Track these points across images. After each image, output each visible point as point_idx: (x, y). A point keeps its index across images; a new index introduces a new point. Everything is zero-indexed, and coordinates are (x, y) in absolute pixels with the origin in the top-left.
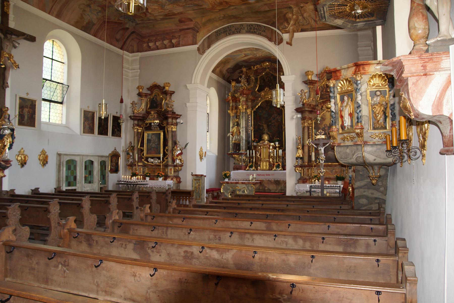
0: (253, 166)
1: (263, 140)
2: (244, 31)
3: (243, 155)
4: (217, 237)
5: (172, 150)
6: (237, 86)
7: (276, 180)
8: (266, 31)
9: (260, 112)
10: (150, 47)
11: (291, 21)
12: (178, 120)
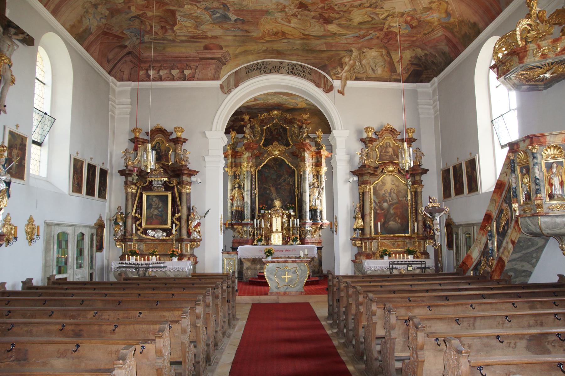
0: (262, 240)
1: (275, 207)
2: (284, 71)
3: (249, 226)
4: (539, 322)
5: (188, 220)
6: (237, 138)
8: (313, 74)
10: (149, 76)
11: (345, 67)
12: (193, 178)
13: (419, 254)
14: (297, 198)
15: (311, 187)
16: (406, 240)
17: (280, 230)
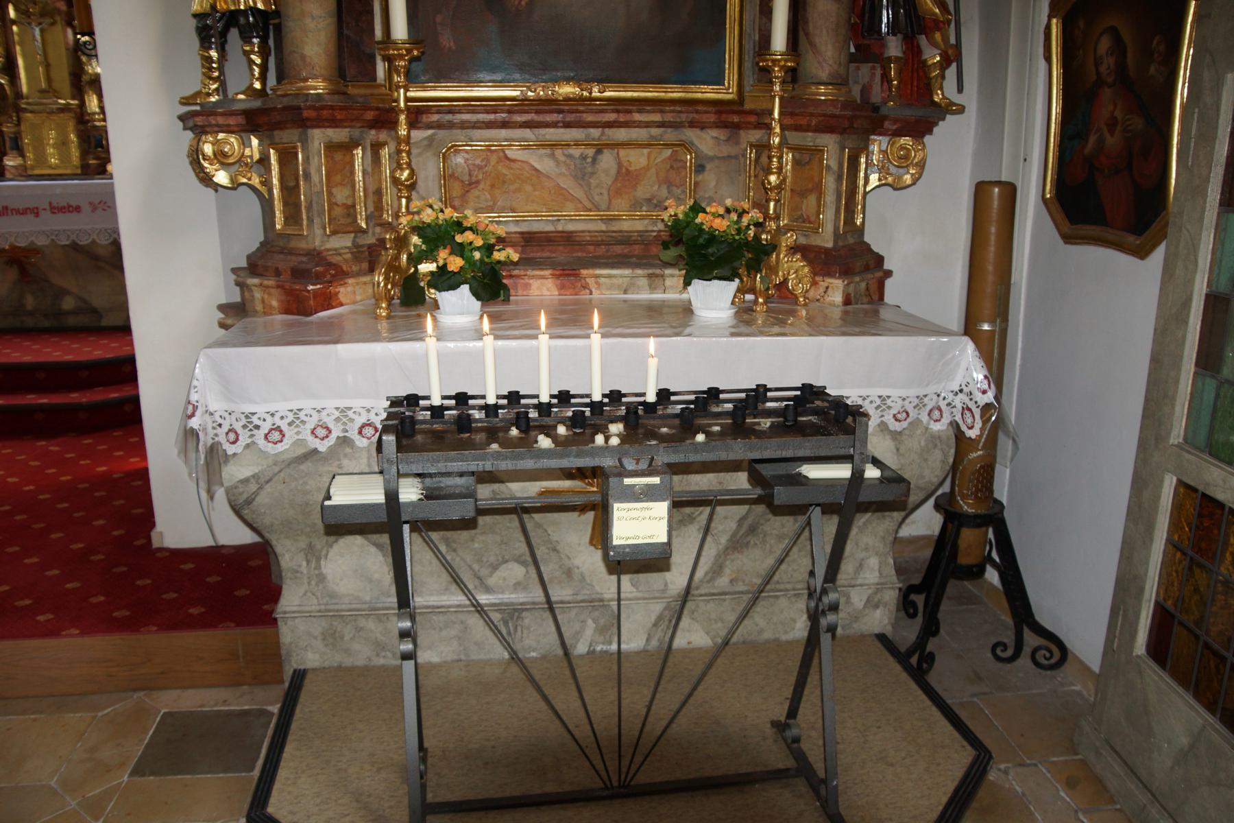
13: (792, 269)
16: (691, 134)
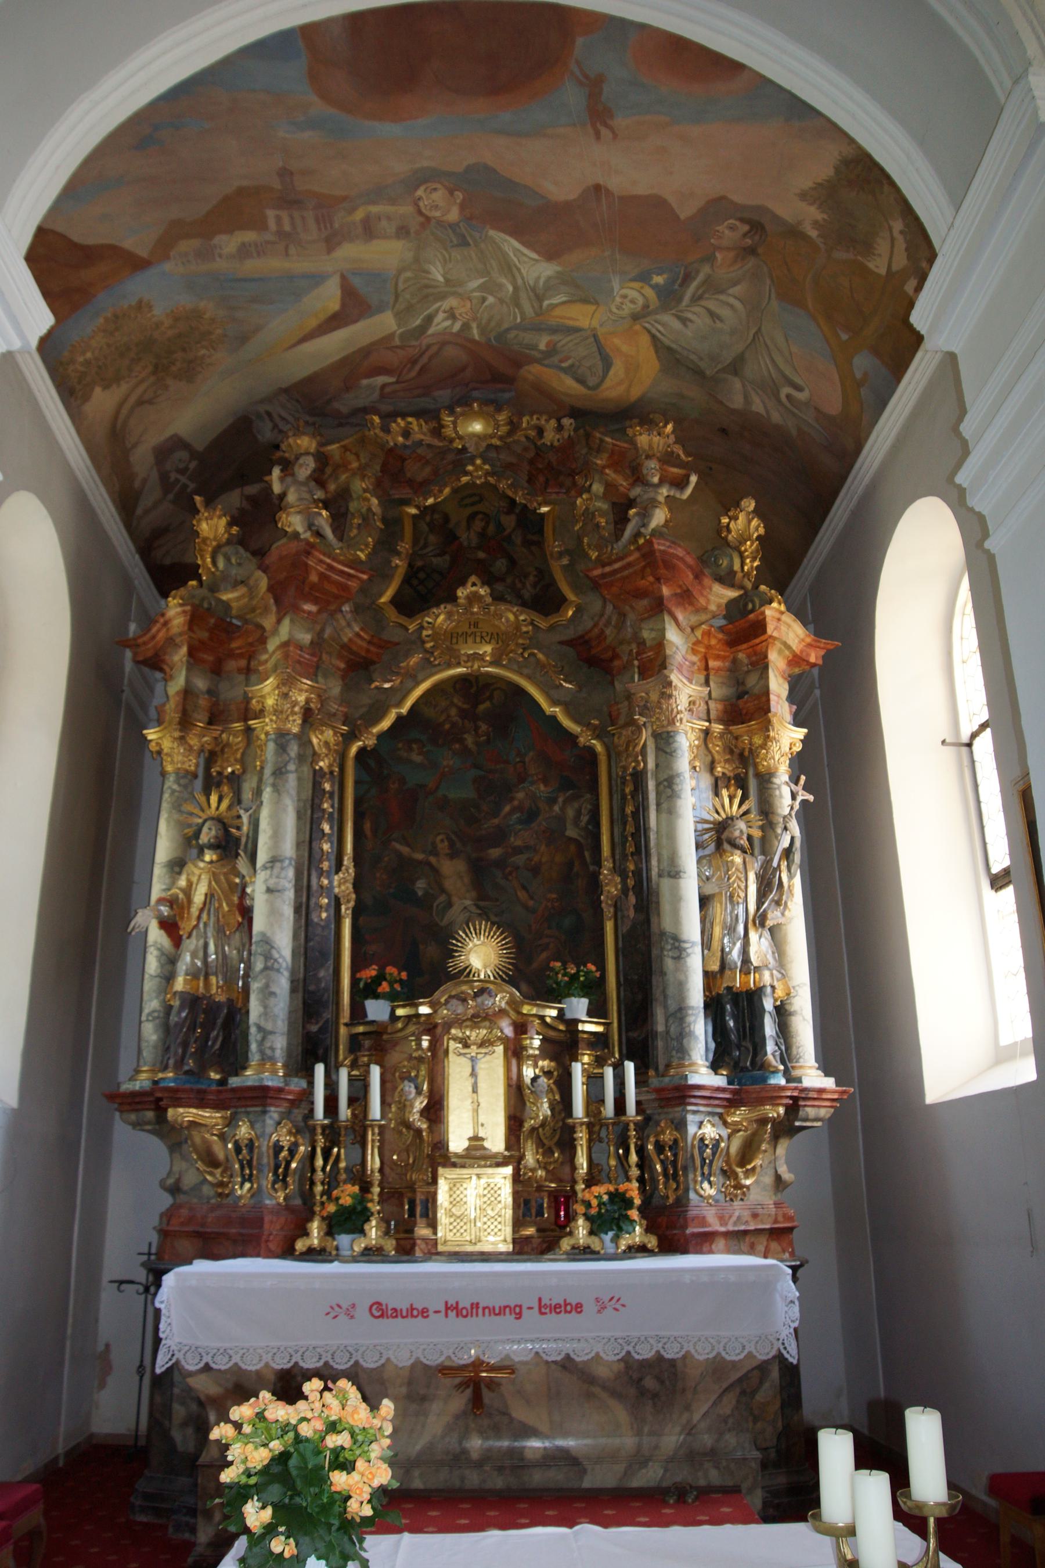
0: (365, 1216)
1: (465, 973)
3: (274, 1113)
7: (644, 1353)
9: (417, 758)
14: (609, 926)
15: (707, 851)
17: (496, 1142)
